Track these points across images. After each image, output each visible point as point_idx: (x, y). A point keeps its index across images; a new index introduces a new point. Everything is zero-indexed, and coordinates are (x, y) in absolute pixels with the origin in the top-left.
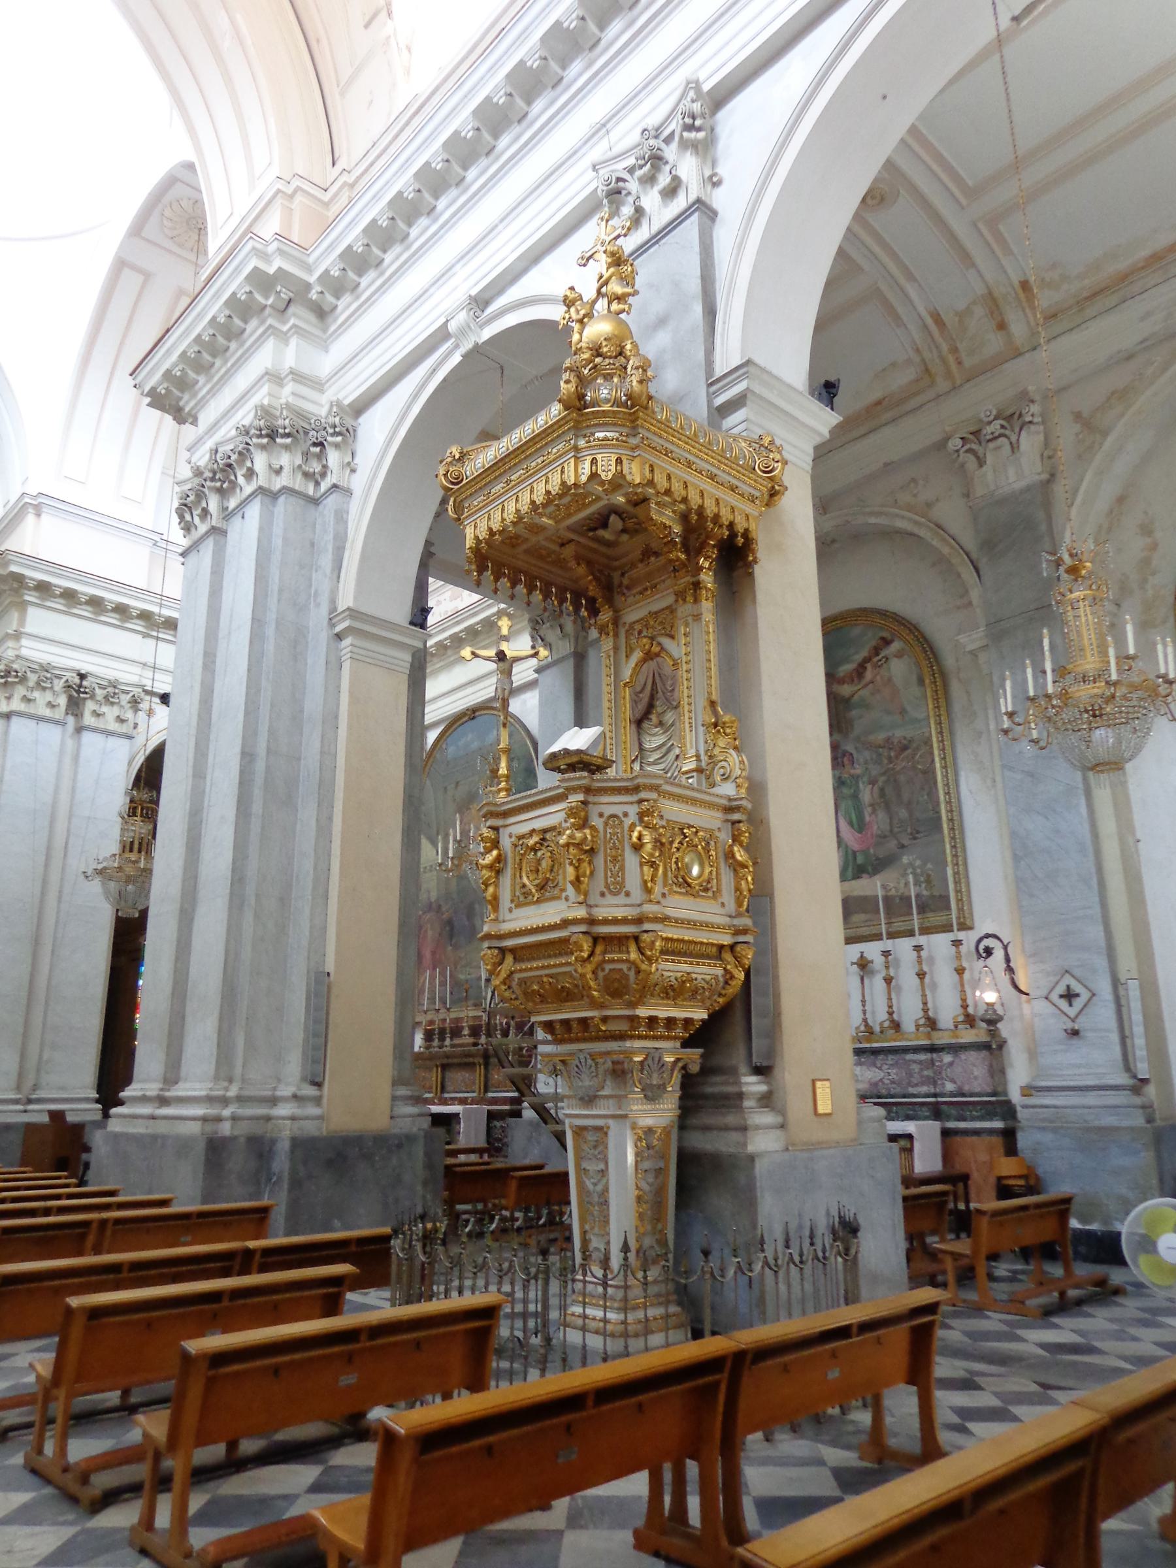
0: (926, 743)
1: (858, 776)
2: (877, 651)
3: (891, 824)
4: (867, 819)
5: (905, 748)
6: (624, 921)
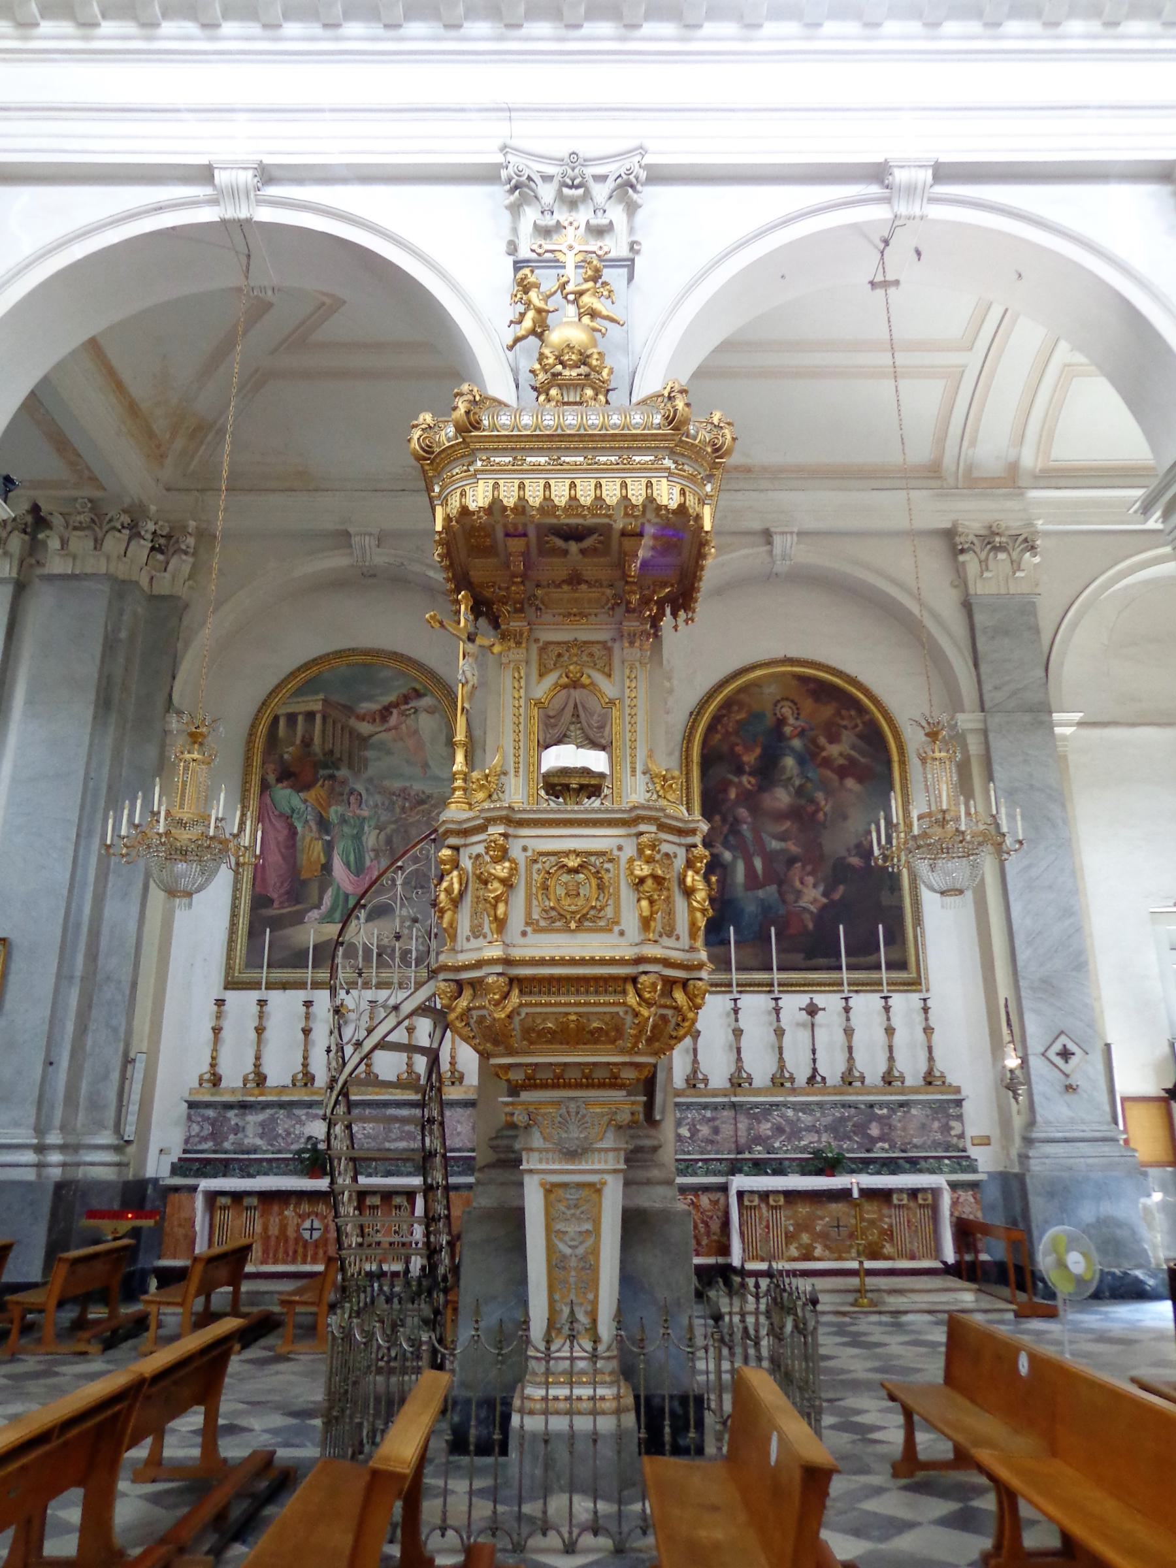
1: (364, 819)
2: (406, 699)
4: (368, 863)
6: (622, 962)
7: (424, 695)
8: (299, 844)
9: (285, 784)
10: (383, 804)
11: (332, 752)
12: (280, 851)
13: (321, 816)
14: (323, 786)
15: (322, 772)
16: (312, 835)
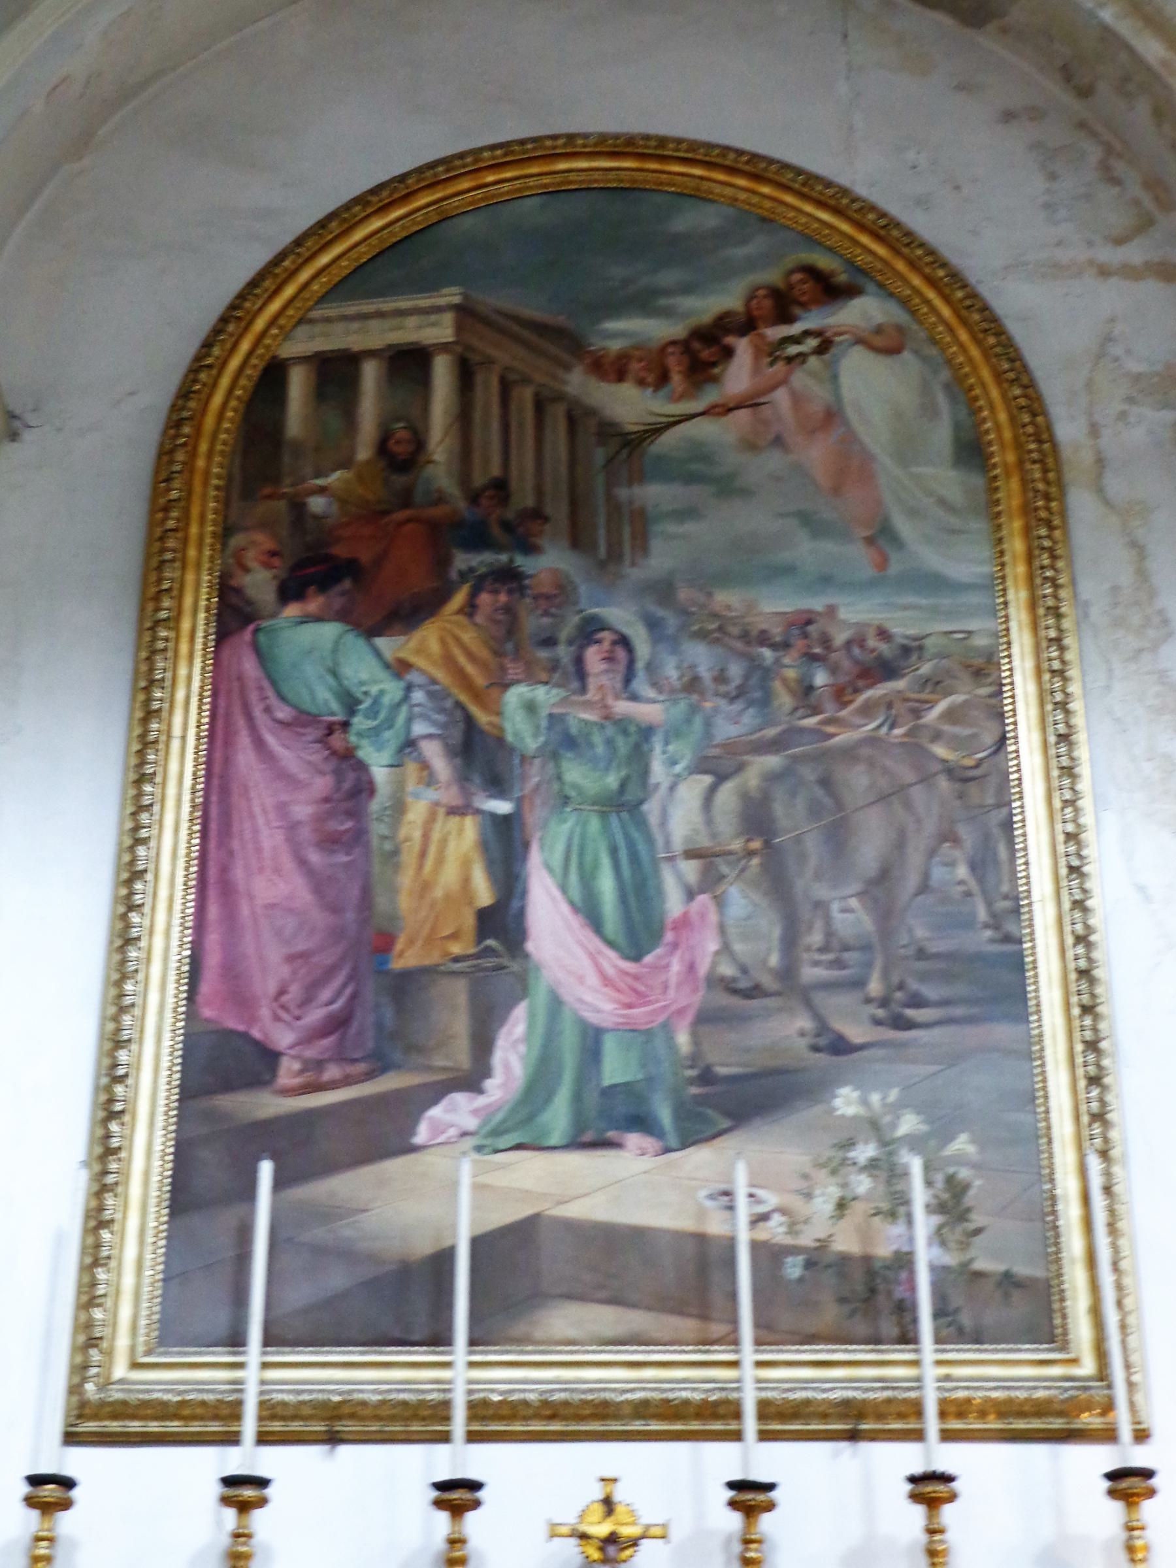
0: (978, 674)
1: (647, 732)
3: (790, 942)
4: (674, 904)
5: (886, 670)
7: (849, 292)
8: (378, 829)
9: (314, 604)
10: (721, 678)
11: (500, 487)
12: (302, 862)
13: (469, 722)
14: (470, 609)
15: (462, 560)
16: (432, 795)
